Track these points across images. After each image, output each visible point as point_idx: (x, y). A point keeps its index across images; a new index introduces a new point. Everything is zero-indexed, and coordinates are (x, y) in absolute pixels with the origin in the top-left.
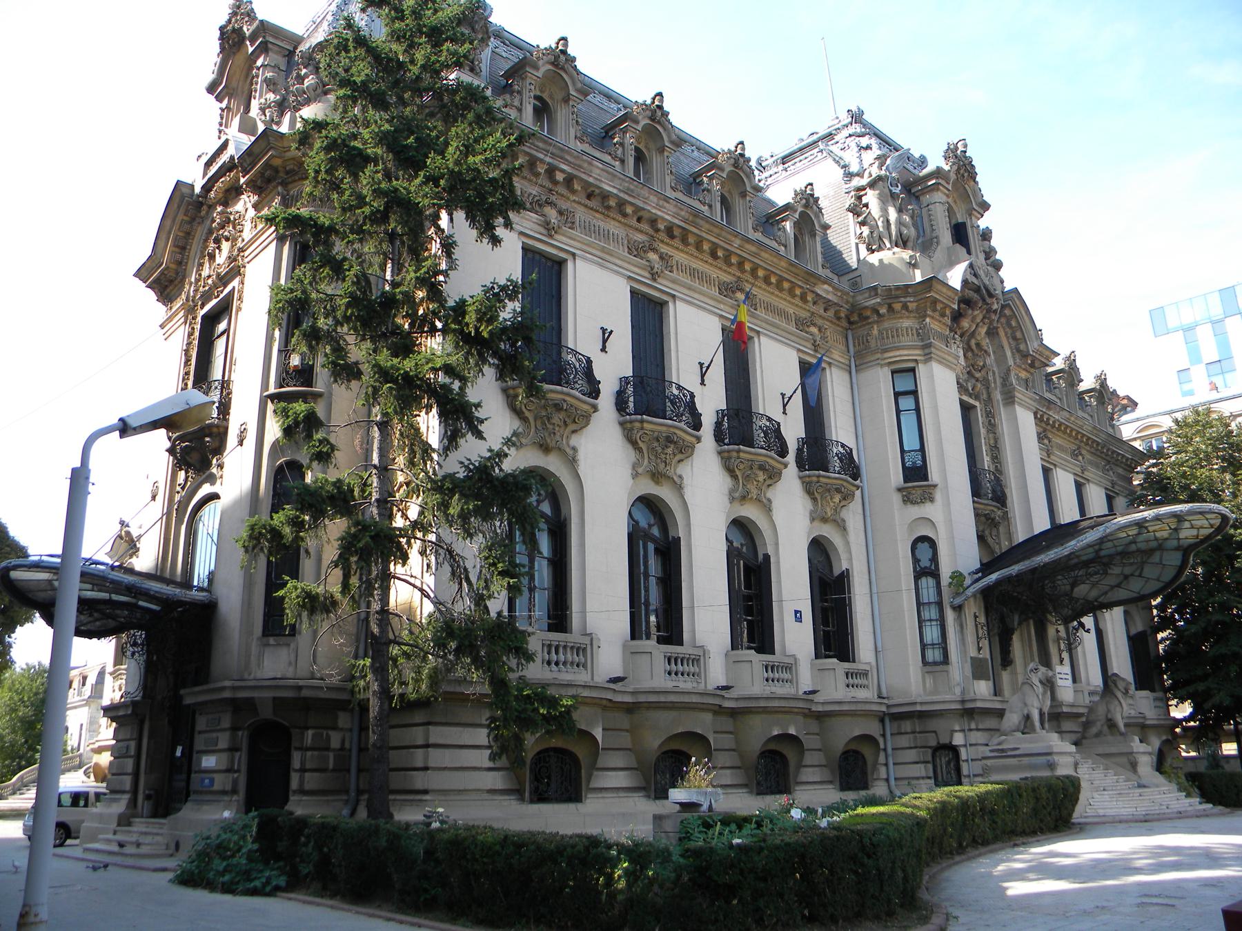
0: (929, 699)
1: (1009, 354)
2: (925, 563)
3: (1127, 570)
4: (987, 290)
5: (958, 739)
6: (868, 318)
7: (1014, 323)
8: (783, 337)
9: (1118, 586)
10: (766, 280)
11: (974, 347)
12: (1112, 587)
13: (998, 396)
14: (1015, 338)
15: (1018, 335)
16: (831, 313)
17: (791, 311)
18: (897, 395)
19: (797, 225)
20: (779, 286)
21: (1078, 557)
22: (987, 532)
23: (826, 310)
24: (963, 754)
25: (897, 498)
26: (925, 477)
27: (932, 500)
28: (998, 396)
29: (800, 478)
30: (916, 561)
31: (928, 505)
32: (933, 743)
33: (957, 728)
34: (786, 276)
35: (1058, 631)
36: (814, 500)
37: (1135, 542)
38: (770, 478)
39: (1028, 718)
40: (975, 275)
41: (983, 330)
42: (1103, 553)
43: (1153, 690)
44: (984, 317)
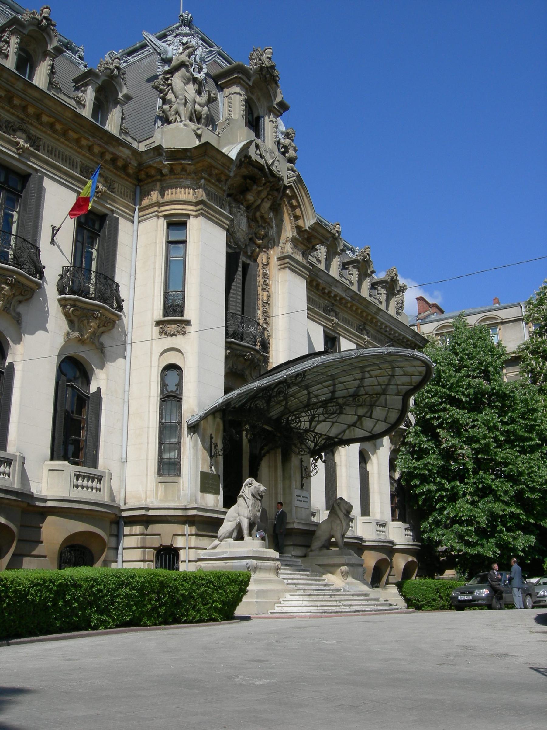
0: (156, 504)
2: (172, 388)
5: (180, 542)
6: (153, 176)
7: (294, 203)
8: (68, 181)
9: (354, 425)
10: (52, 126)
12: (349, 426)
15: (298, 212)
17: (78, 160)
18: (169, 242)
19: (99, 91)
20: (64, 134)
21: (316, 396)
22: (247, 372)
24: (182, 555)
25: (156, 330)
26: (182, 315)
27: (184, 333)
29: (59, 300)
30: (164, 385)
31: (180, 337)
32: (158, 545)
33: (180, 533)
35: (302, 461)
37: (363, 386)
38: (21, 294)
39: (239, 527)
40: (261, 155)
41: (267, 205)
42: (337, 394)
43: (404, 522)
44: (268, 194)
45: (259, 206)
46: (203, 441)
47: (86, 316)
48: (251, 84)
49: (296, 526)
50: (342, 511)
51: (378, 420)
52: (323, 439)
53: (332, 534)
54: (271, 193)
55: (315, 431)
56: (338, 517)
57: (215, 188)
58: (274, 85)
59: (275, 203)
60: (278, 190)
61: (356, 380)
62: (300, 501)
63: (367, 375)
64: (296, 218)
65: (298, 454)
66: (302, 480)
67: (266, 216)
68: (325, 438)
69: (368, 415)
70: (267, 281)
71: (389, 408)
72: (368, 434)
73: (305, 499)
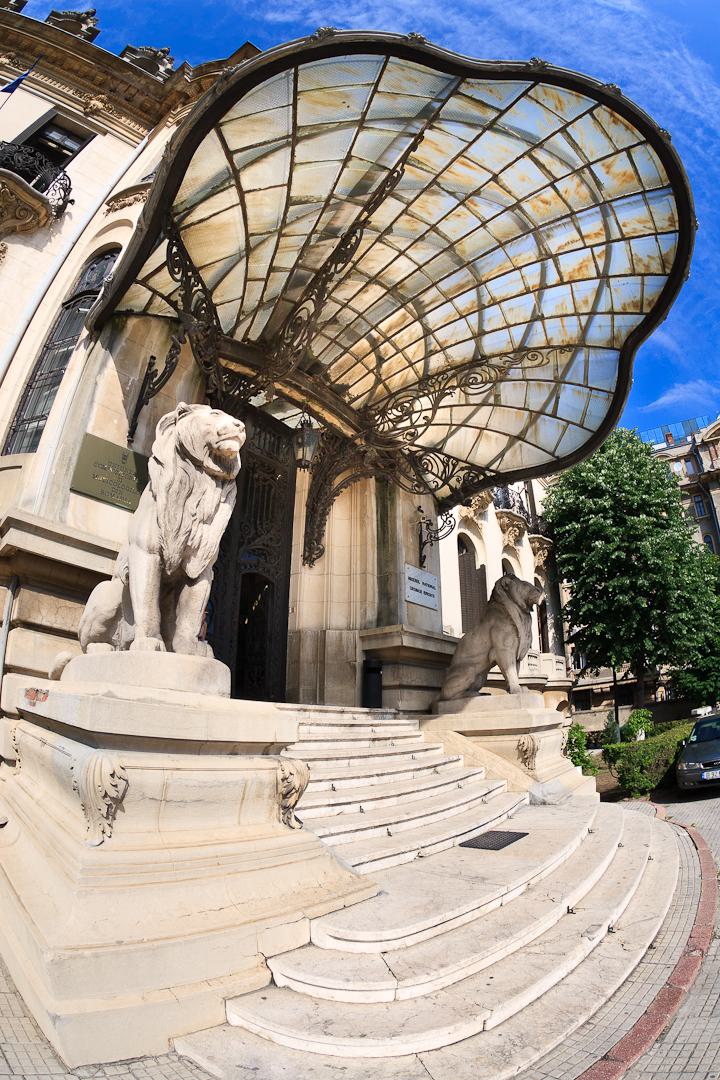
3: (537, 400)
37: (542, 318)
46: (121, 367)
49: (407, 641)
50: (516, 603)
51: (568, 422)
52: (462, 469)
53: (493, 657)
55: (446, 451)
56: (509, 615)
61: (528, 291)
62: (417, 590)
63: (552, 277)
66: (421, 550)
69: (549, 410)
72: (547, 458)
73: (430, 590)
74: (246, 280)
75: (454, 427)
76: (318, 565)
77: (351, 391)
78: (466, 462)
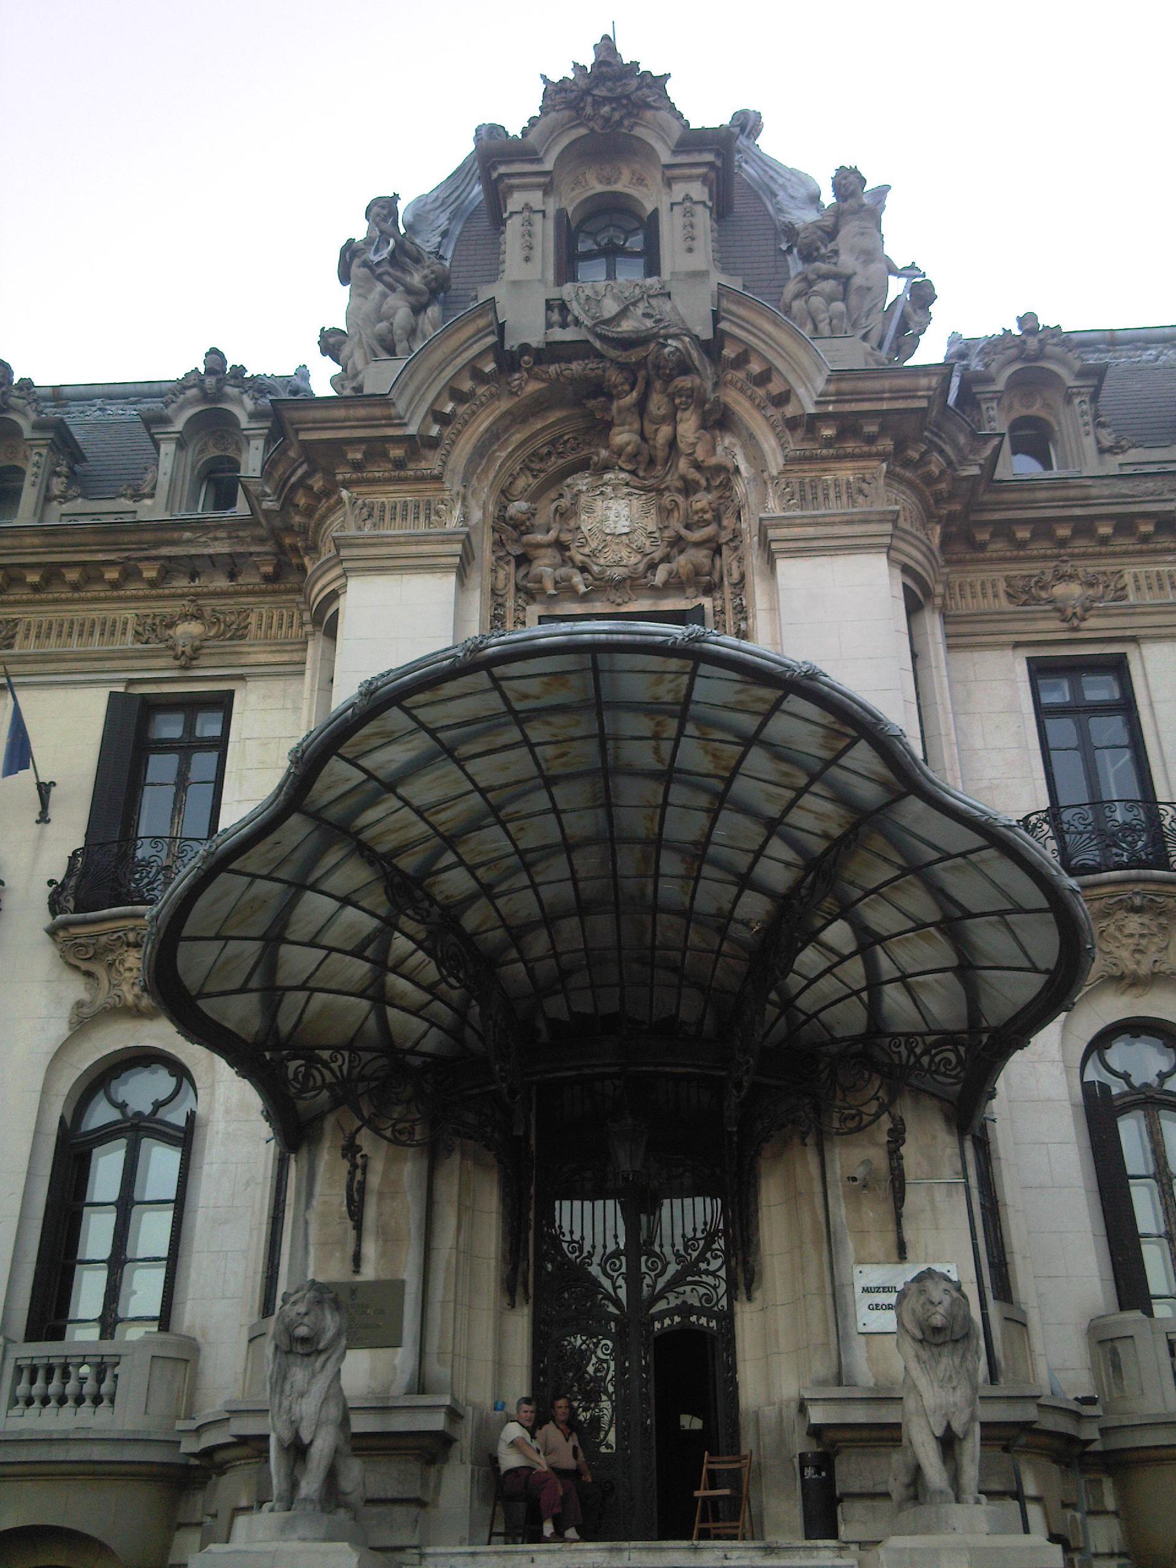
1: (769, 443)
4: (602, 338)
11: (693, 474)
13: (754, 561)
14: (782, 399)
15: (775, 387)
16: (250, 579)
23: (232, 576)
28: (754, 561)
33: (244, 1503)
34: (101, 557)
36: (89, 974)
41: (688, 426)
44: (671, 396)
45: (672, 443)
47: (112, 950)
48: (548, 166)
54: (670, 390)
57: (406, 487)
58: (649, 114)
59: (707, 406)
60: (684, 367)
64: (782, 399)
65: (858, 1127)
67: (700, 455)
68: (936, 1044)
70: (743, 626)
71: (963, 855)
72: (1037, 981)
74: (415, 1013)
75: (864, 995)
76: (757, 1294)
77: (683, 1015)
78: (931, 1032)
